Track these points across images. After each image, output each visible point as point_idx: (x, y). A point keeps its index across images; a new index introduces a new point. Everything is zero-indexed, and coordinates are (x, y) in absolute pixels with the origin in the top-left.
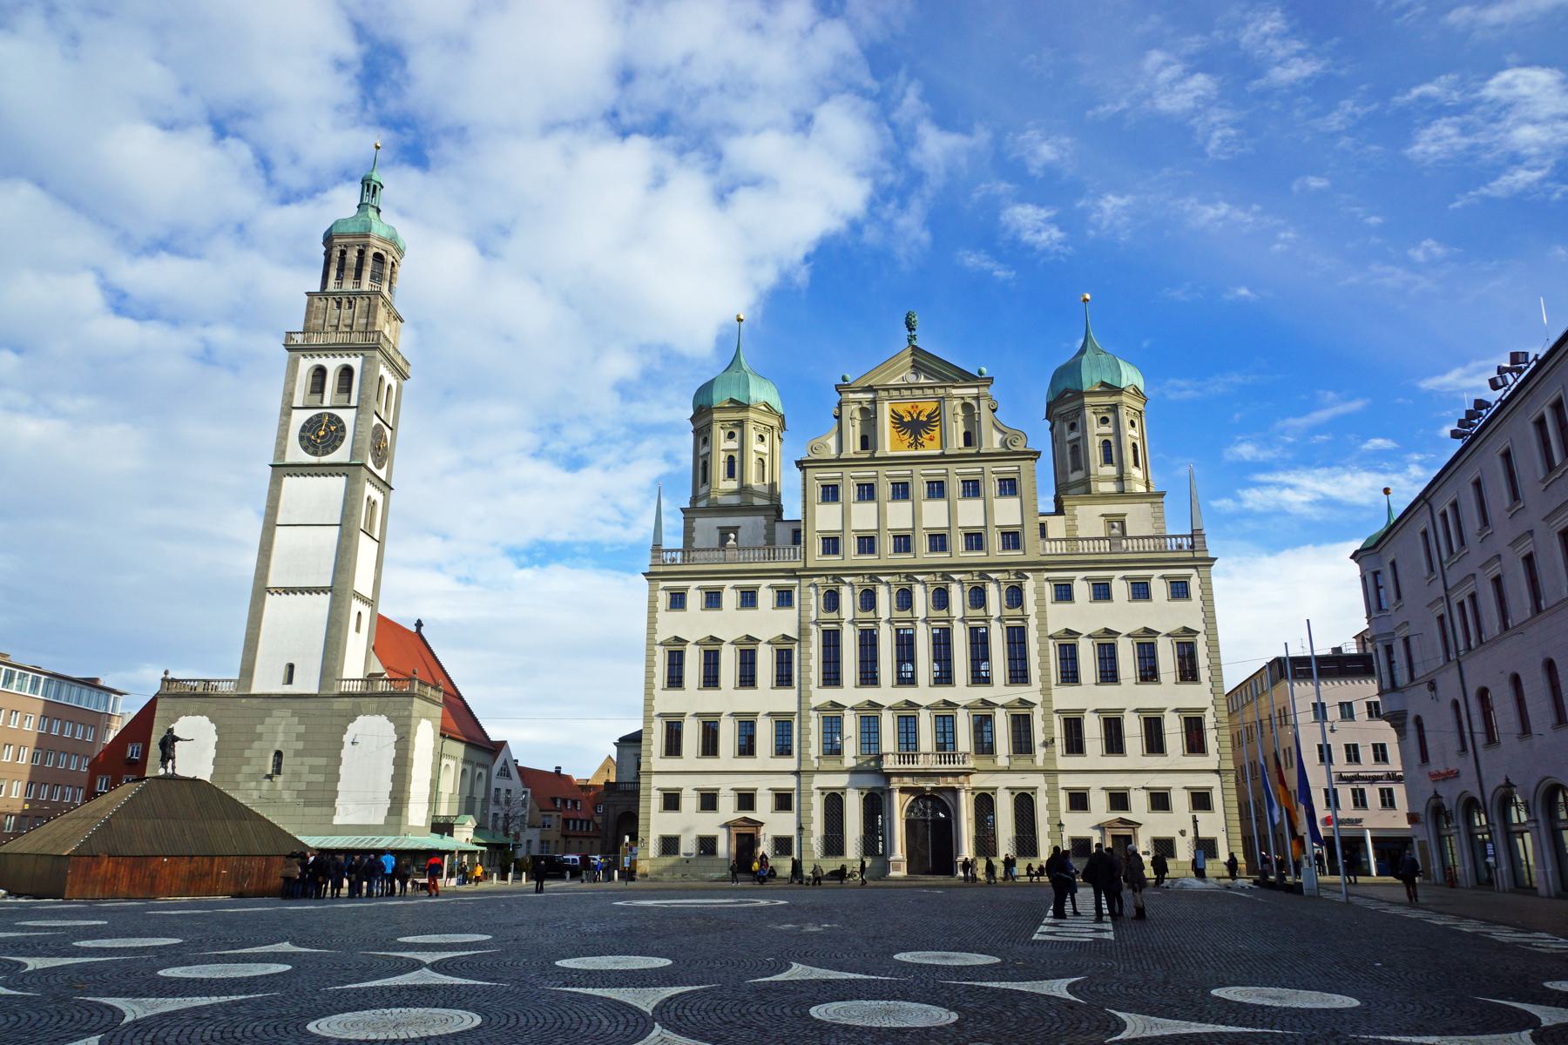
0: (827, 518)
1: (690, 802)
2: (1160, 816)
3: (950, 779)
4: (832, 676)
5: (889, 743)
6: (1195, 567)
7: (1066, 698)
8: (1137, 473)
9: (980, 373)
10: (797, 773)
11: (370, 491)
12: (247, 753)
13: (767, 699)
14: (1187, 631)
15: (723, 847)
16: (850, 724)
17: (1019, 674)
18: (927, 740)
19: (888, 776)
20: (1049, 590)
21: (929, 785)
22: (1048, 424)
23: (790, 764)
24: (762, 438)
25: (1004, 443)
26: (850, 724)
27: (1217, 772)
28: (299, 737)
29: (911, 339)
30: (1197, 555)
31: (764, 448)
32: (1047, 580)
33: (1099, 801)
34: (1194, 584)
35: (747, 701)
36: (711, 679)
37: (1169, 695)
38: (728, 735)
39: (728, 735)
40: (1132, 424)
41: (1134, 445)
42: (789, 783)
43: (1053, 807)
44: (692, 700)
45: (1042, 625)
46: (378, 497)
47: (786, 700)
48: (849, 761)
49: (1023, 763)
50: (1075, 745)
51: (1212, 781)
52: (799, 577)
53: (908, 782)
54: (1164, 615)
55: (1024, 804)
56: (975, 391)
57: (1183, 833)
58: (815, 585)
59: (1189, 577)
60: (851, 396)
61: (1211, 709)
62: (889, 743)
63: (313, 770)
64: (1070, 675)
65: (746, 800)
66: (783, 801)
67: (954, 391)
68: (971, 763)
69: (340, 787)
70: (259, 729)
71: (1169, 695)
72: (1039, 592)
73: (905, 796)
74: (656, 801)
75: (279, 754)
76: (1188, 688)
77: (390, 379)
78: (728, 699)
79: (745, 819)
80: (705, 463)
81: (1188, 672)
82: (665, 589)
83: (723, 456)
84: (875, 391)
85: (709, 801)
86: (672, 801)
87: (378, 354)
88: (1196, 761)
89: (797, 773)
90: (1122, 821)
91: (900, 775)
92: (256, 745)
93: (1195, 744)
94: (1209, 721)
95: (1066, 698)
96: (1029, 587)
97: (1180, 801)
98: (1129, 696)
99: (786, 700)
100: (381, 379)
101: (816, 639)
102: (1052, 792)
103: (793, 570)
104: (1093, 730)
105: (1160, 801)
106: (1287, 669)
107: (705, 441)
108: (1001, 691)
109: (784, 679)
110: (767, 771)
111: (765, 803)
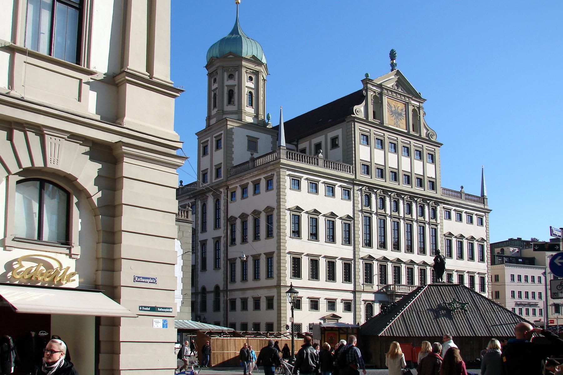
5: (390, 280)
6: (485, 212)
10: (354, 292)
14: (483, 239)
18: (404, 280)
23: (350, 287)
32: (444, 208)
34: (484, 219)
36: (314, 236)
42: (350, 296)
45: (442, 229)
48: (376, 288)
52: (354, 184)
58: (361, 190)
62: (390, 280)
65: (332, 304)
66: (348, 306)
82: (289, 175)
85: (315, 304)
89: (354, 292)
99: (347, 252)
103: (353, 180)
109: (348, 240)
111: (340, 307)
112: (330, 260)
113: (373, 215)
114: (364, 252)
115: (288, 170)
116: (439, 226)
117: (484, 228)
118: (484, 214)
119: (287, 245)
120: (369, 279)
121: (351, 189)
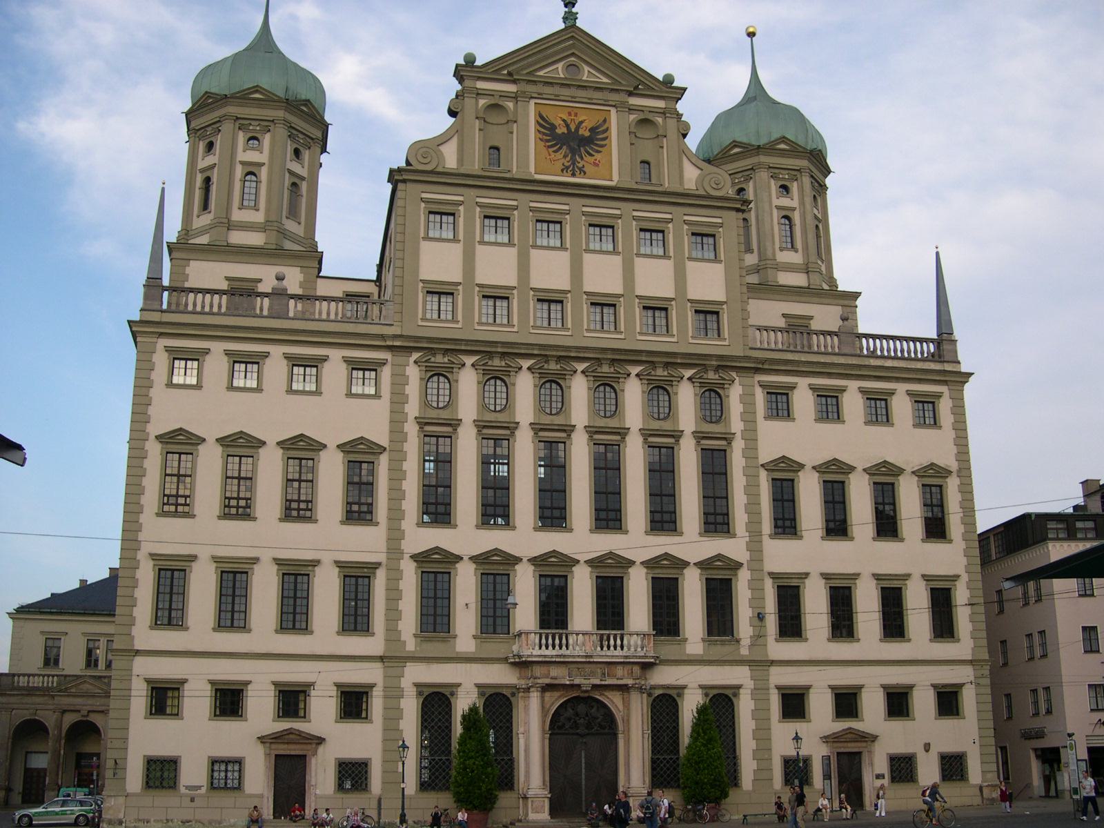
0: (438, 260)
1: (197, 701)
2: (897, 725)
4: (438, 508)
6: (945, 382)
7: (783, 556)
9: (669, 80)
13: (330, 540)
15: (258, 780)
16: (466, 586)
17: (717, 520)
19: (522, 664)
20: (760, 396)
21: (585, 682)
23: (372, 645)
24: (297, 153)
25: (700, 180)
26: (466, 586)
27: (971, 662)
29: (570, 17)
30: (948, 367)
31: (303, 172)
33: (821, 705)
34: (945, 406)
35: (298, 541)
37: (914, 558)
38: (265, 594)
39: (265, 594)
41: (817, 226)
43: (761, 715)
44: (205, 536)
47: (365, 543)
49: (720, 651)
50: (791, 626)
51: (962, 675)
53: (561, 675)
54: (906, 444)
55: (720, 705)
56: (661, 104)
57: (927, 747)
59: (939, 396)
60: (481, 85)
61: (965, 578)
62: (525, 614)
64: (786, 524)
65: (292, 700)
66: (353, 703)
67: (634, 101)
68: (648, 651)
71: (914, 558)
72: (748, 400)
73: (548, 694)
74: (139, 701)
76: (936, 547)
78: (267, 538)
79: (290, 732)
80: (208, 180)
81: (936, 528)
83: (239, 171)
84: (515, 82)
85: (229, 701)
86: (163, 699)
88: (944, 650)
90: (850, 731)
93: (943, 627)
94: (961, 595)
95: (783, 556)
96: (735, 394)
97: (923, 702)
98: (864, 556)
101: (412, 446)
102: (760, 692)
103: (383, 337)
104: (816, 605)
105: (898, 702)
107: (210, 146)
108: (691, 544)
109: (358, 510)
110: (327, 654)
112: (292, 570)
113: (461, 430)
114: (422, 538)
115: (161, 335)
116: (738, 446)
117: (947, 432)
118: (943, 389)
119: (141, 537)
120: (435, 616)
121: (383, 363)
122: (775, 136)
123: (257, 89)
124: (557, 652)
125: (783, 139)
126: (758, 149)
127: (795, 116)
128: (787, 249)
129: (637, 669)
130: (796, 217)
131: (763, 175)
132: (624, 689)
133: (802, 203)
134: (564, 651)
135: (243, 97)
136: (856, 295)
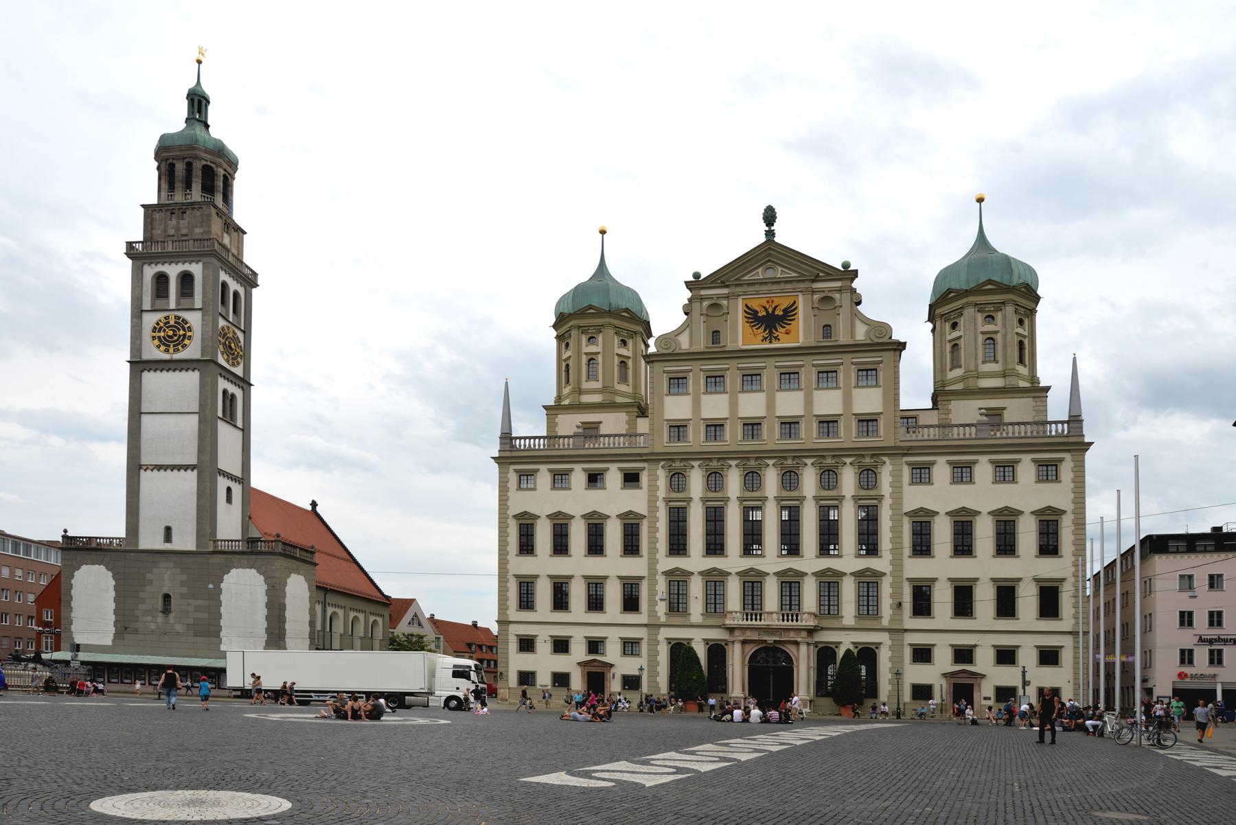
3: (792, 634)
8: (1023, 370)
11: (223, 384)
12: (141, 595)
21: (770, 639)
22: (930, 326)
28: (183, 584)
40: (1021, 322)
41: (1021, 343)
43: (896, 659)
46: (232, 389)
63: (197, 609)
69: (222, 623)
70: (149, 576)
75: (167, 597)
77: (233, 286)
87: (214, 261)
91: (743, 629)
92: (148, 588)
100: (224, 286)
106: (1156, 545)
122: (983, 279)
123: (590, 307)
124: (749, 622)
125: (990, 282)
126: (967, 293)
127: (1007, 261)
128: (990, 362)
129: (804, 634)
130: (999, 338)
131: (969, 312)
132: (797, 643)
133: (1004, 325)
134: (754, 622)
135: (581, 313)
136: (1047, 389)
